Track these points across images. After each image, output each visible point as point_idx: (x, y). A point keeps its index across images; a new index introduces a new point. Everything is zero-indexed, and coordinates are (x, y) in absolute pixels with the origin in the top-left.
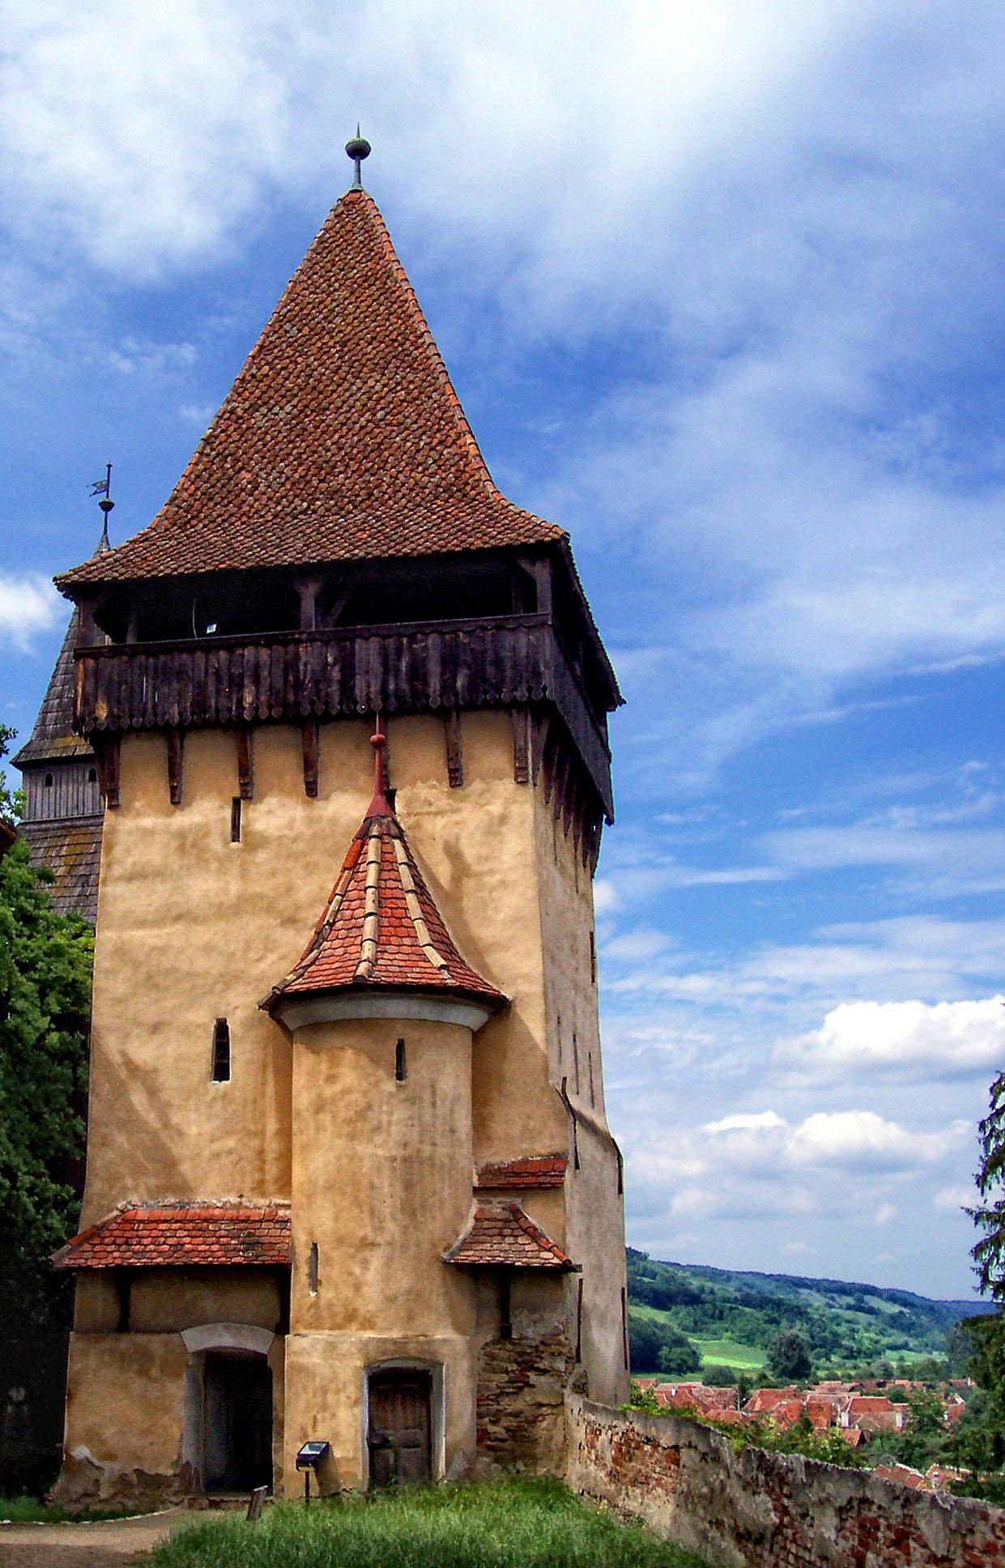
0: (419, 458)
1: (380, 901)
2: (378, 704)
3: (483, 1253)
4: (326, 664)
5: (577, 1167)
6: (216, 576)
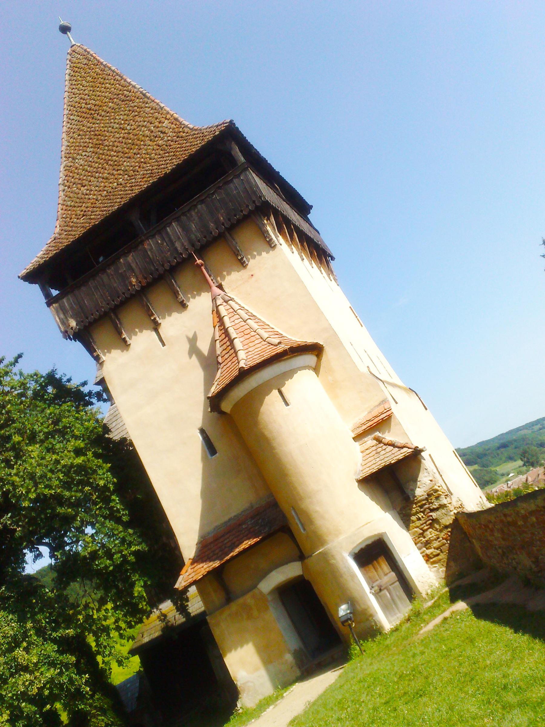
3: (374, 466)
5: (397, 403)
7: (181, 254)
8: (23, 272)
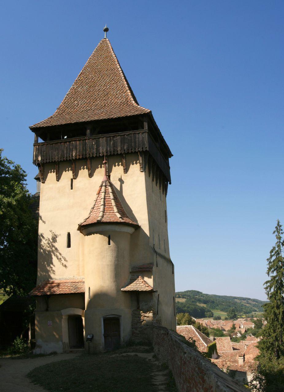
0: (117, 96)
1: (104, 202)
2: (105, 154)
4: (93, 144)
5: (157, 266)
6: (66, 125)
7: (100, 153)
8: (32, 125)
